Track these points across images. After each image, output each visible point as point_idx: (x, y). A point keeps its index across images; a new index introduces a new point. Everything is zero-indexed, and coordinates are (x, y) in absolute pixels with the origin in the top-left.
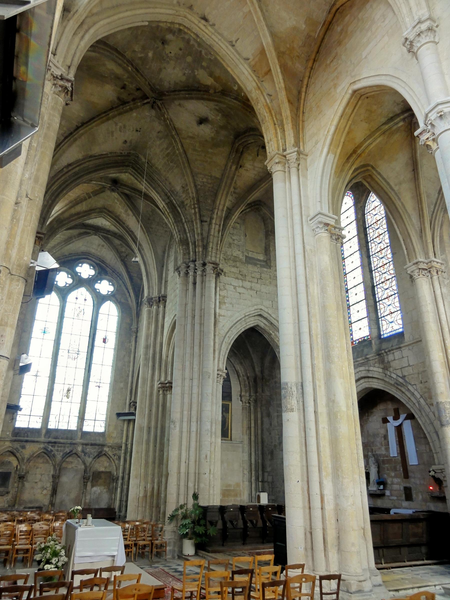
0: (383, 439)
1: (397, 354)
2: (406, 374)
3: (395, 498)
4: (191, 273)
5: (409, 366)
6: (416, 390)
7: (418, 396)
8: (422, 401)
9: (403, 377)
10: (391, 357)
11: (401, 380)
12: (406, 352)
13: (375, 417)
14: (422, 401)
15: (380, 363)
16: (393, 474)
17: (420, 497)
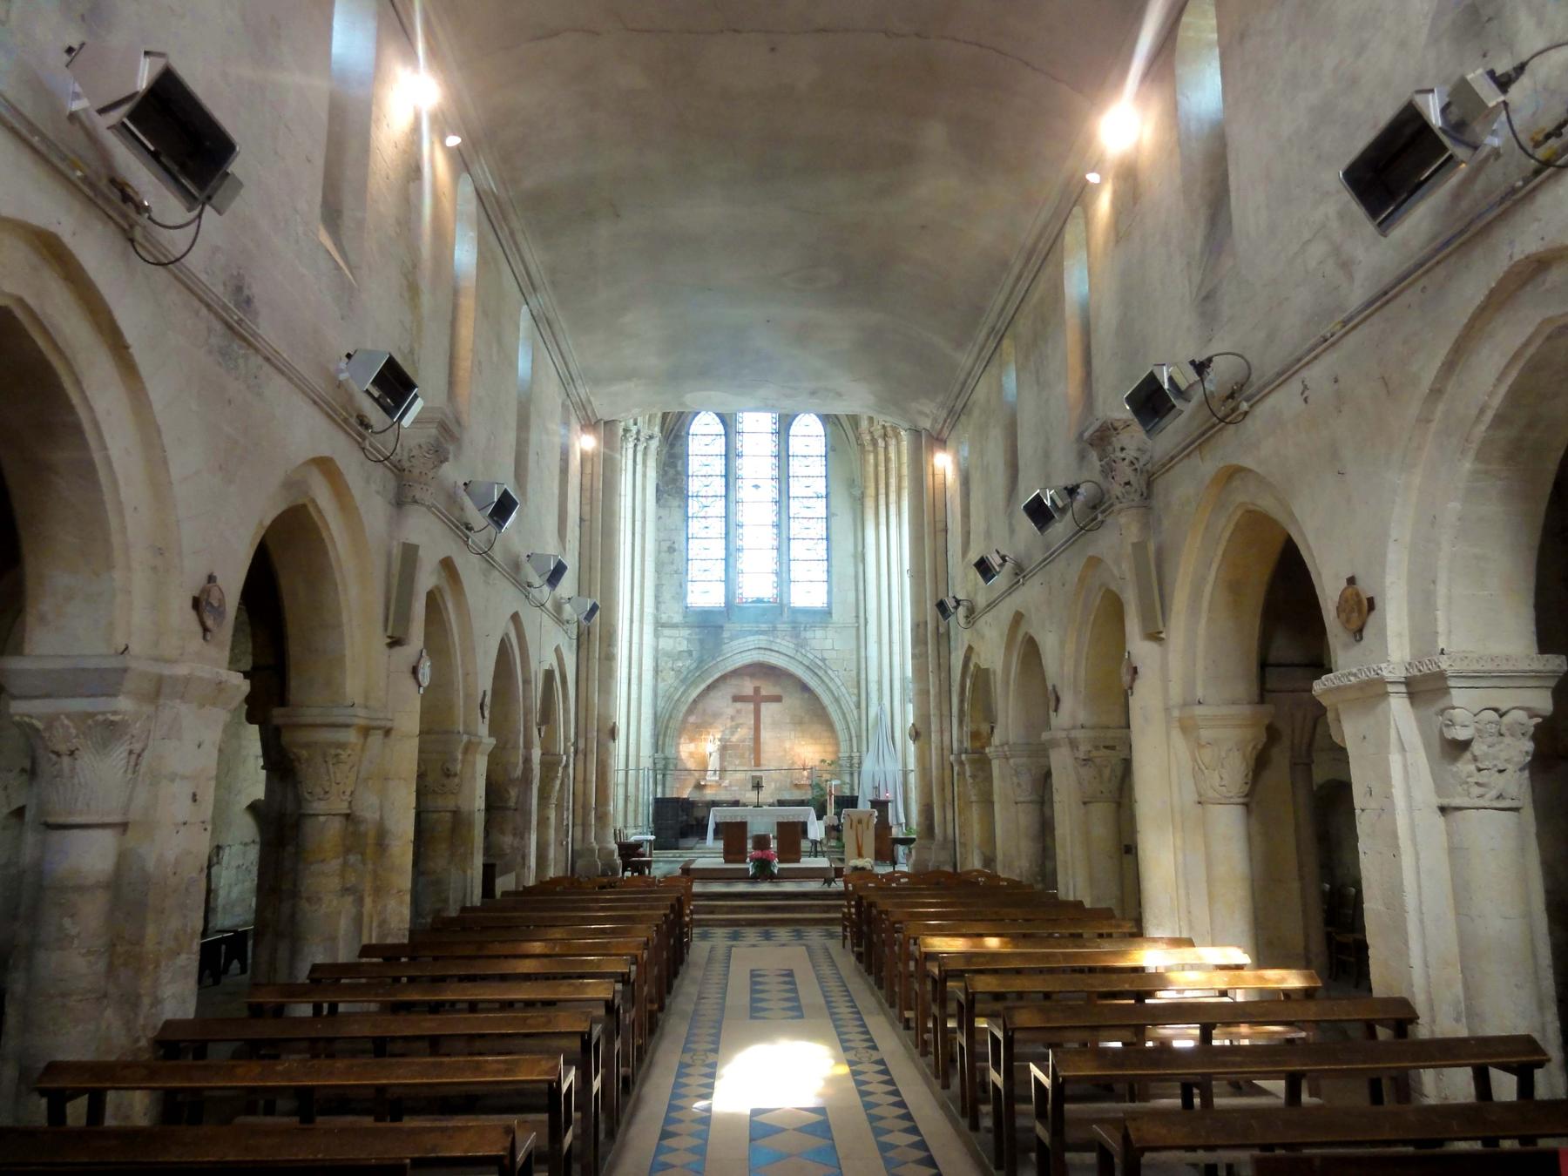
0: (729, 721)
1: (819, 633)
2: (826, 656)
3: (736, 788)
4: (631, 445)
5: (833, 649)
6: (838, 677)
7: (840, 684)
8: (843, 689)
9: (823, 660)
10: (809, 634)
11: (820, 663)
12: (831, 633)
13: (720, 694)
14: (843, 689)
15: (792, 637)
16: (737, 762)
17: (773, 785)
